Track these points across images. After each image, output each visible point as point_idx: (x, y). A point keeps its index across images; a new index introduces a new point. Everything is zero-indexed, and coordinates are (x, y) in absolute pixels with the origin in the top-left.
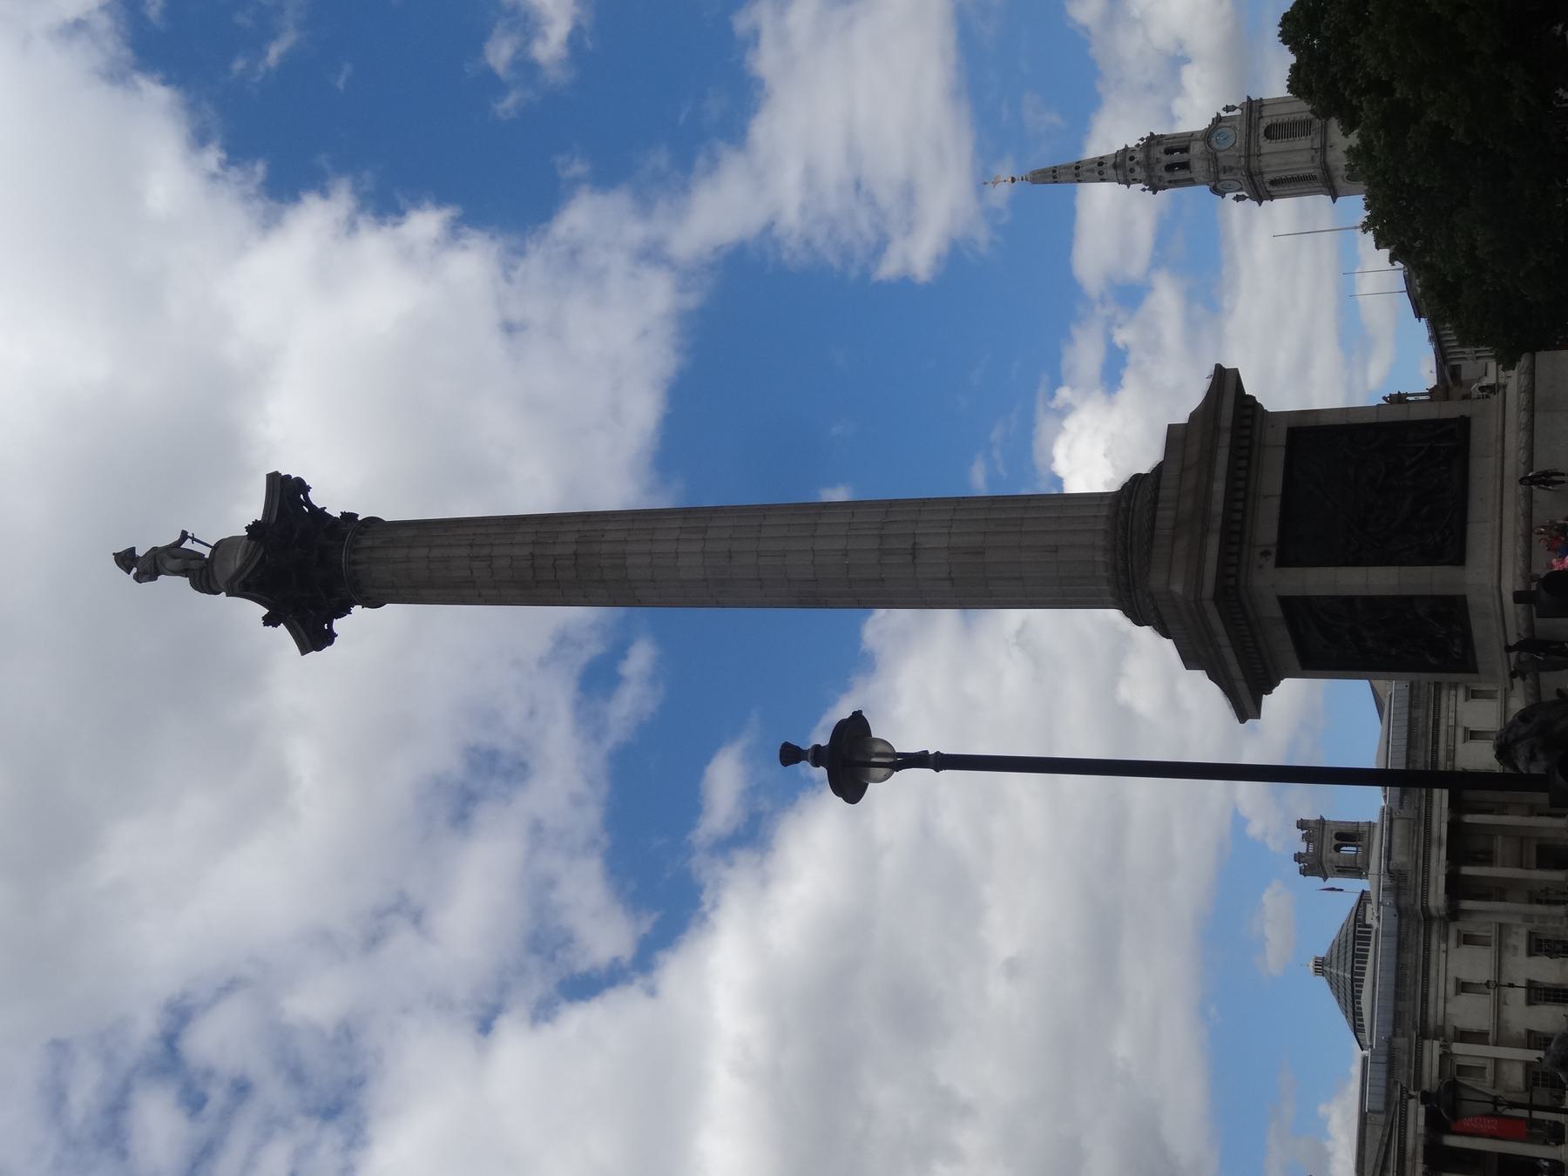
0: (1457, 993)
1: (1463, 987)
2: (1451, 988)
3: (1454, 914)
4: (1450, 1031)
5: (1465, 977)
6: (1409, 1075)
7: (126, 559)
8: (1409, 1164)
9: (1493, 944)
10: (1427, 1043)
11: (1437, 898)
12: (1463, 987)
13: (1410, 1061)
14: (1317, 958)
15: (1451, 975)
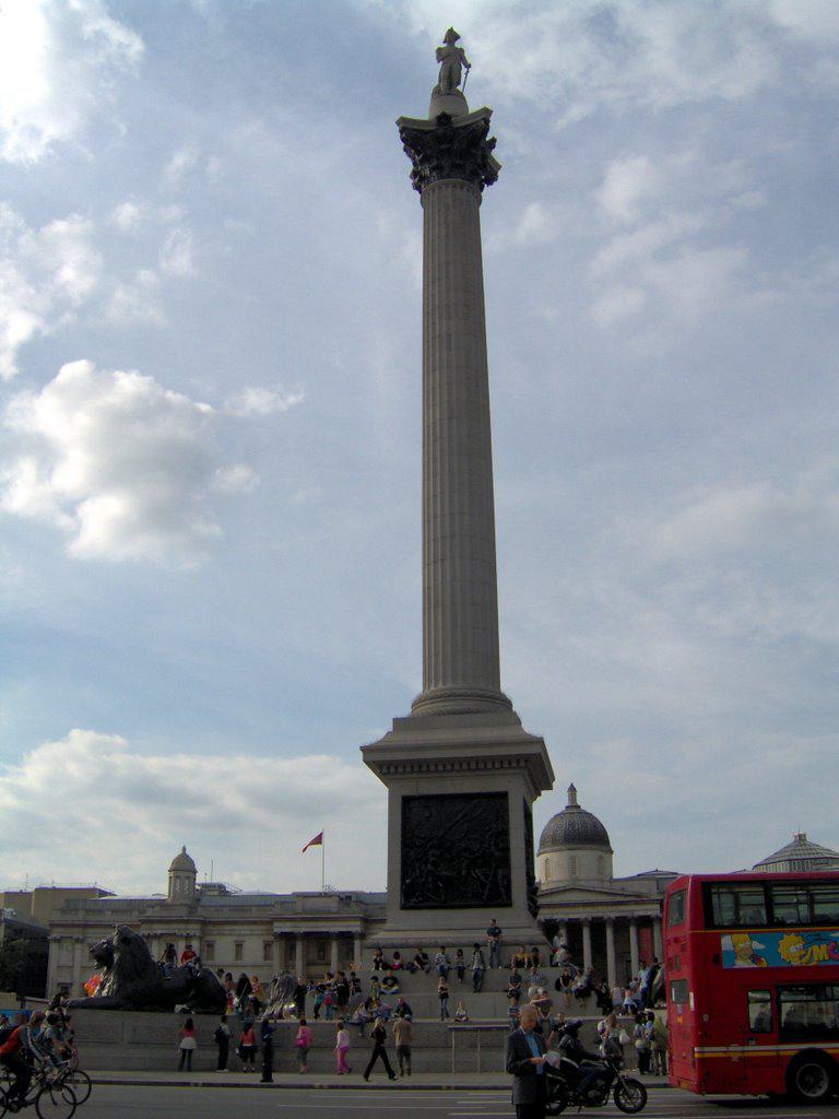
8: (614, 908)
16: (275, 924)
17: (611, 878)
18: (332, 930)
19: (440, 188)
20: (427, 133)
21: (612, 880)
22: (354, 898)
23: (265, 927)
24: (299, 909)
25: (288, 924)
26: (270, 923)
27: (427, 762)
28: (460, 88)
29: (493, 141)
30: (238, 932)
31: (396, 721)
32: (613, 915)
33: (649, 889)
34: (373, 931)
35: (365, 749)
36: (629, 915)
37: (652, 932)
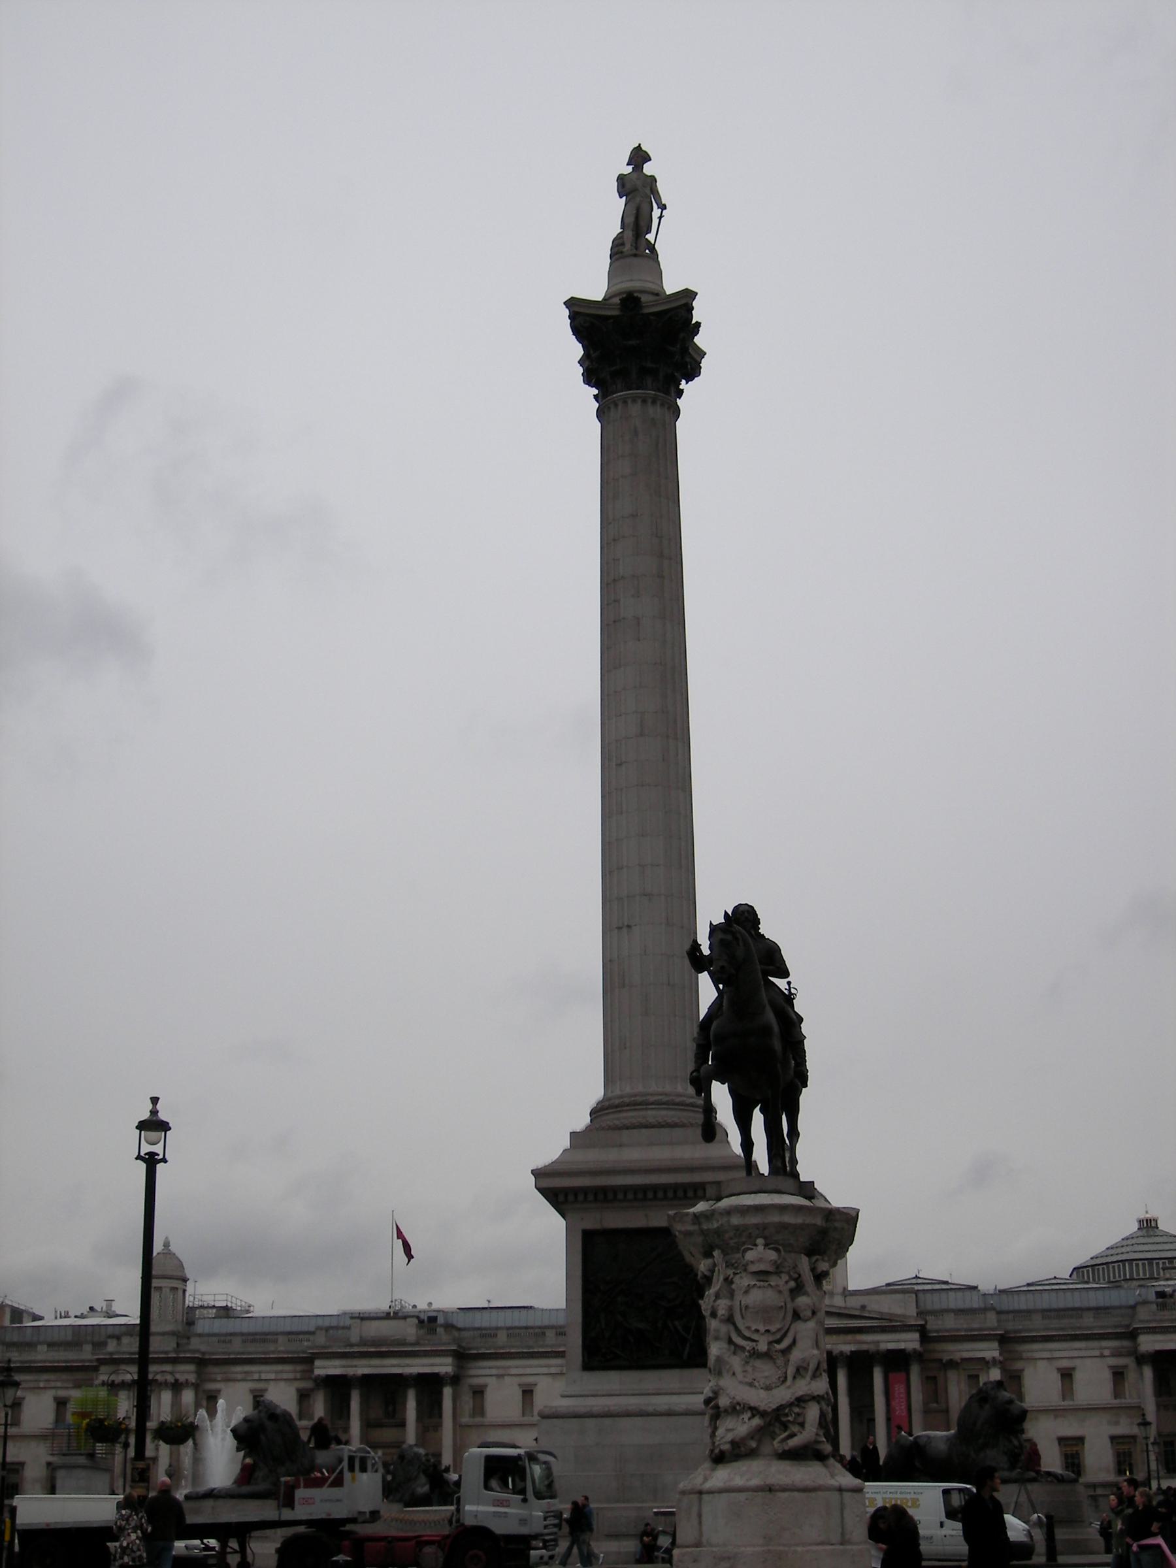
0: (1059, 1369)
1: (1067, 1375)
2: (1065, 1364)
3: (1141, 1359)
4: (1019, 1365)
5: (1078, 1376)
6: (958, 1330)
7: (639, 157)
8: (849, 1337)
9: (1118, 1401)
10: (995, 1345)
11: (1149, 1343)
12: (1067, 1375)
13: (972, 1330)
14: (1156, 1221)
15: (1077, 1362)
16: (317, 1363)
17: (845, 1289)
18: (407, 1371)
19: (625, 402)
20: (607, 318)
21: (846, 1293)
22: (441, 1320)
23: (299, 1368)
24: (355, 1338)
25: (337, 1362)
26: (309, 1360)
27: (615, 1190)
28: (650, 237)
29: (698, 324)
30: (256, 1377)
31: (573, 1135)
32: (847, 1348)
33: (906, 1309)
34: (472, 1372)
35: (537, 1174)
36: (872, 1348)
37: (908, 1374)
